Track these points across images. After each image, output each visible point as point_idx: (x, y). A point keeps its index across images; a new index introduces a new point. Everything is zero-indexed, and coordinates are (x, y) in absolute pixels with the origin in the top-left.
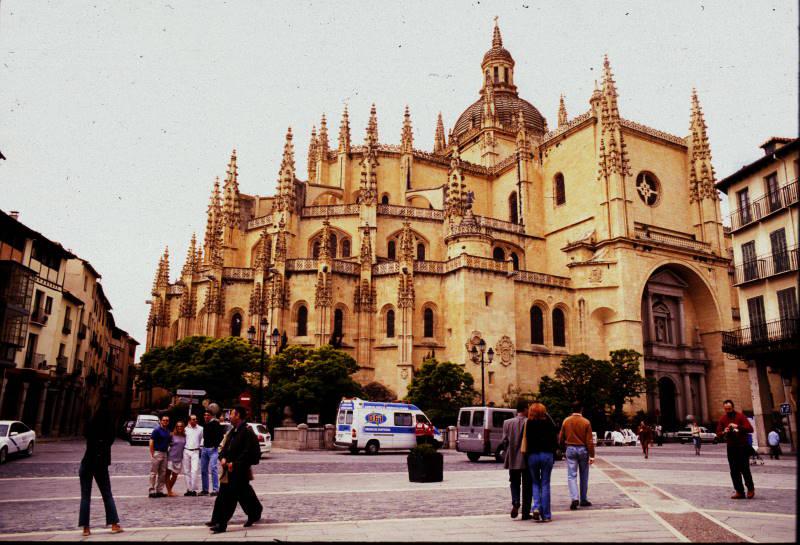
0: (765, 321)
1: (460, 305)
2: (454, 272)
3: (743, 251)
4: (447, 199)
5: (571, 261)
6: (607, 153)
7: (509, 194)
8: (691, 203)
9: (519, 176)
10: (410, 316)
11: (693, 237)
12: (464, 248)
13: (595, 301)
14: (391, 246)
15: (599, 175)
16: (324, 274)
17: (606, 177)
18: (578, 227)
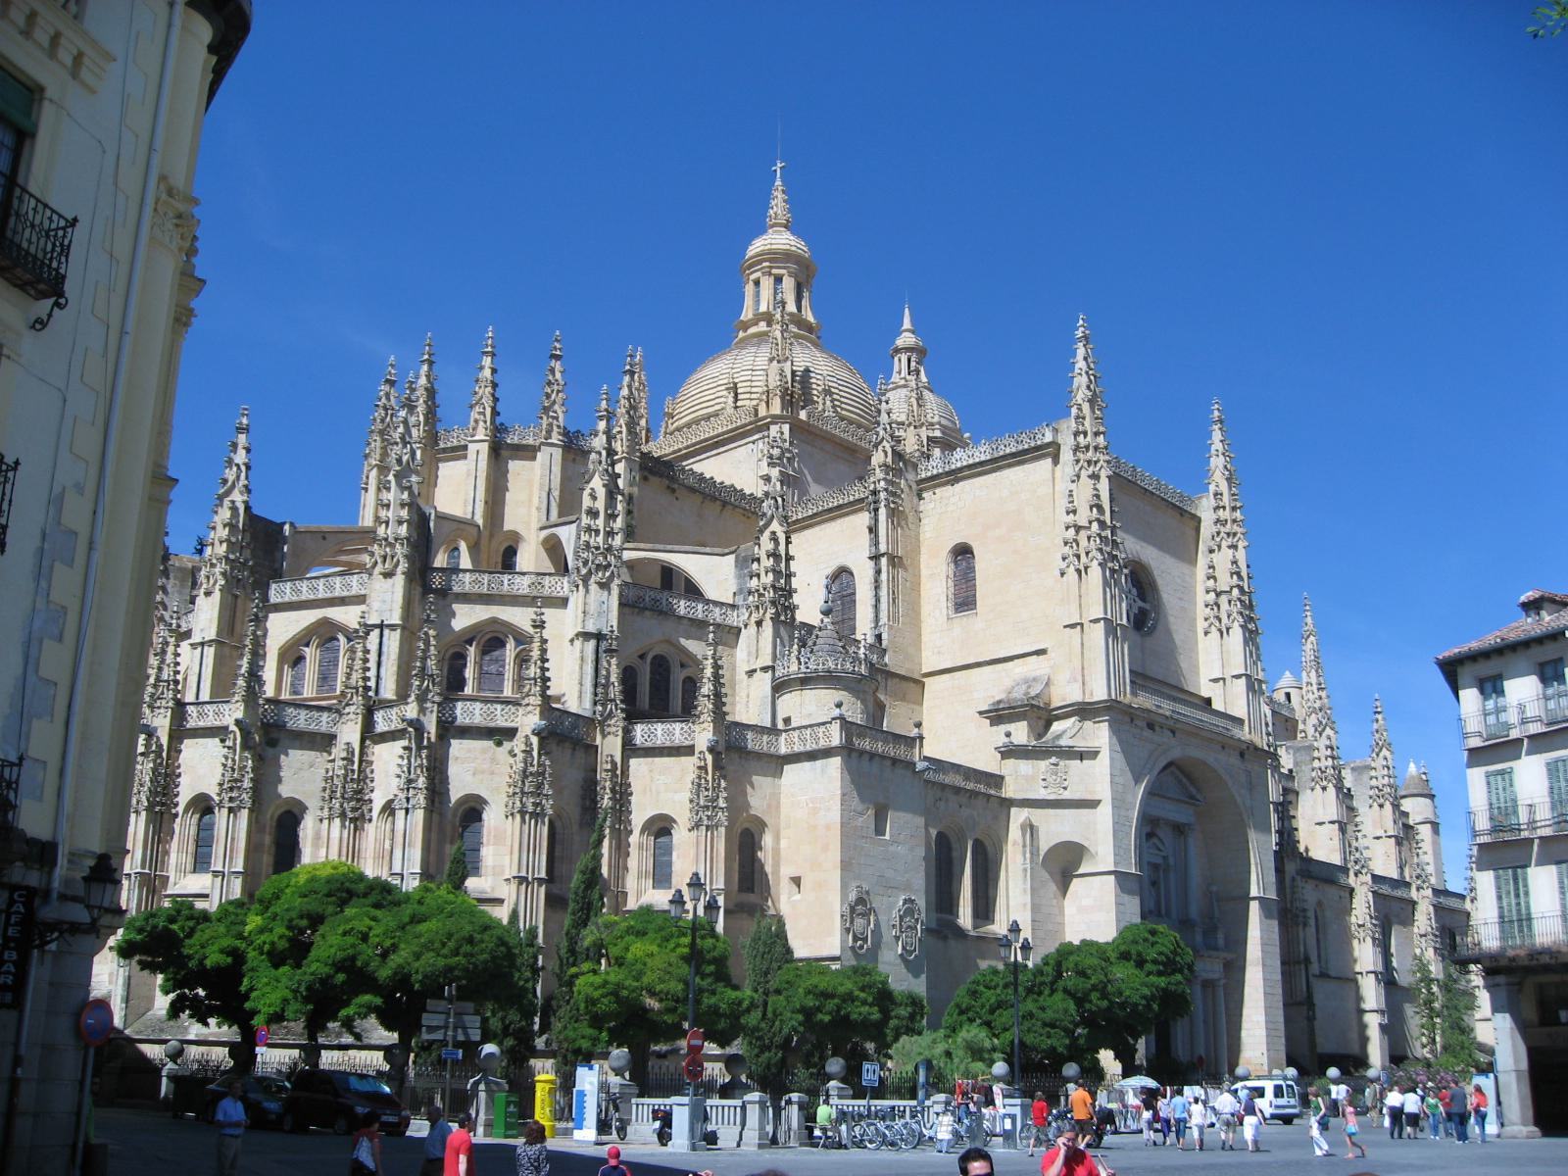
0: (1529, 914)
1: (828, 827)
2: (811, 756)
3: (1488, 783)
4: (754, 582)
5: (1006, 740)
6: (1084, 523)
7: (830, 571)
8: (1206, 633)
9: (876, 544)
10: (721, 846)
11: (1208, 701)
12: (839, 705)
13: (1056, 828)
14: (628, 676)
15: (1063, 565)
16: (535, 740)
17: (1079, 571)
18: (1010, 664)
